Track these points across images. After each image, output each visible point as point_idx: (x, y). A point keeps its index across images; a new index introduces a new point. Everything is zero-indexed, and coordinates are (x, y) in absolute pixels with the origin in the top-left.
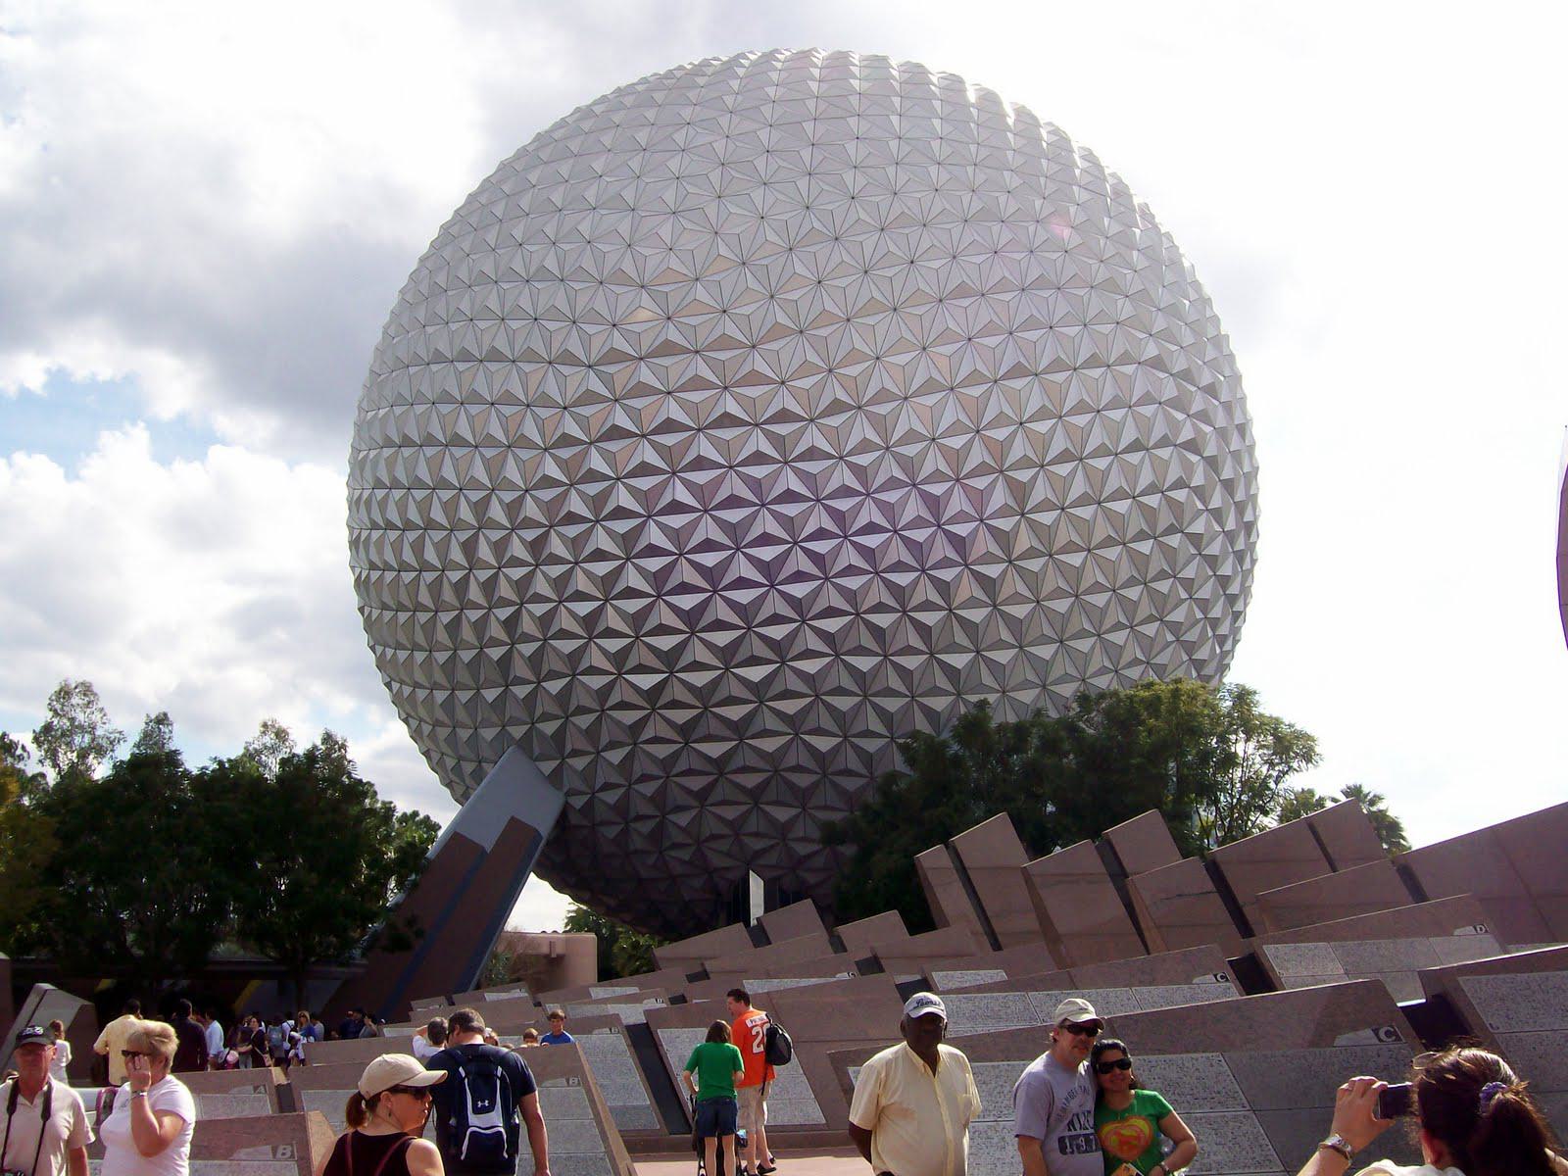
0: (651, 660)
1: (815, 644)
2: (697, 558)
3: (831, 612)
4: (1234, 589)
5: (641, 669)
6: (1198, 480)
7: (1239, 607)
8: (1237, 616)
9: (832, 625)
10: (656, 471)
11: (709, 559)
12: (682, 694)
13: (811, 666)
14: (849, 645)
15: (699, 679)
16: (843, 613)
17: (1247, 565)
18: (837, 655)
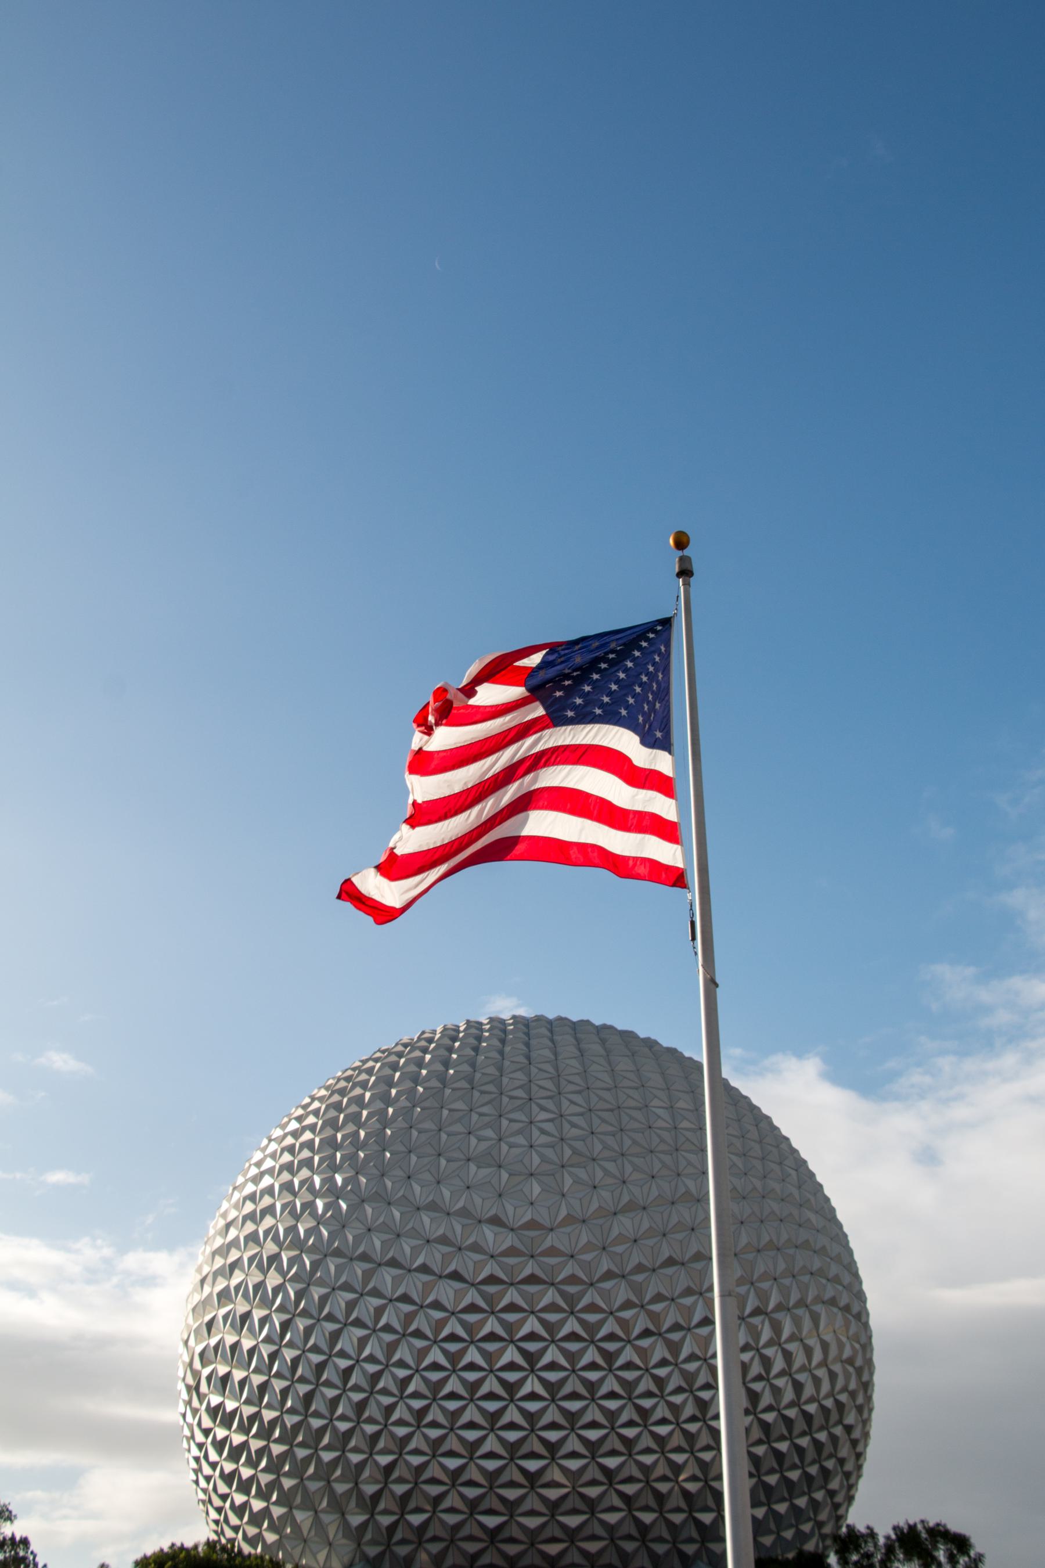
0: (497, 1505)
1: (617, 1502)
2: (545, 1434)
3: (630, 1480)
4: (856, 1434)
5: (491, 1512)
6: (852, 1386)
7: (859, 1449)
8: (859, 1456)
9: (630, 1489)
10: (519, 1368)
11: (553, 1436)
12: (516, 1533)
13: (612, 1518)
14: (641, 1502)
15: (532, 1522)
16: (639, 1481)
17: (865, 1415)
18: (630, 1511)
